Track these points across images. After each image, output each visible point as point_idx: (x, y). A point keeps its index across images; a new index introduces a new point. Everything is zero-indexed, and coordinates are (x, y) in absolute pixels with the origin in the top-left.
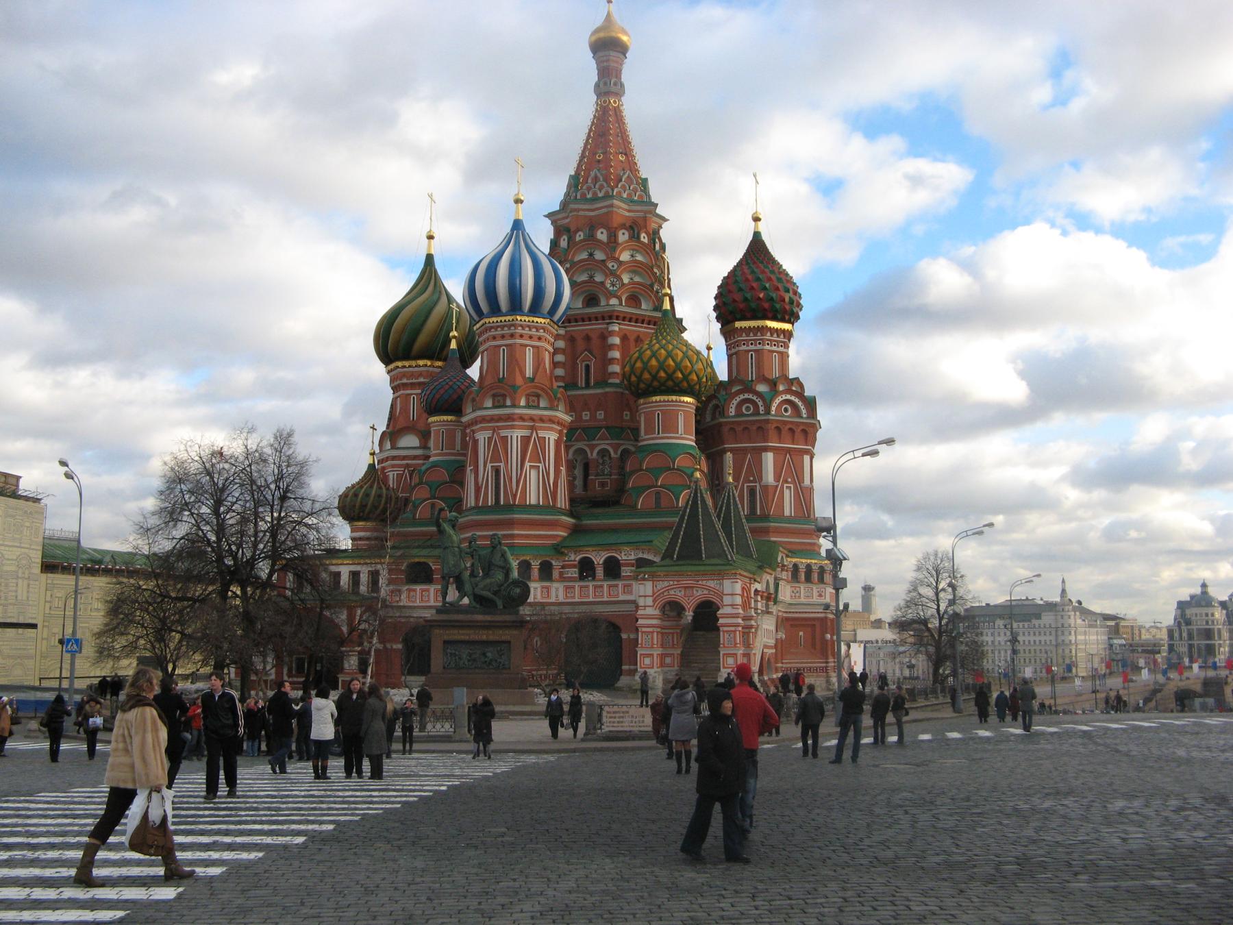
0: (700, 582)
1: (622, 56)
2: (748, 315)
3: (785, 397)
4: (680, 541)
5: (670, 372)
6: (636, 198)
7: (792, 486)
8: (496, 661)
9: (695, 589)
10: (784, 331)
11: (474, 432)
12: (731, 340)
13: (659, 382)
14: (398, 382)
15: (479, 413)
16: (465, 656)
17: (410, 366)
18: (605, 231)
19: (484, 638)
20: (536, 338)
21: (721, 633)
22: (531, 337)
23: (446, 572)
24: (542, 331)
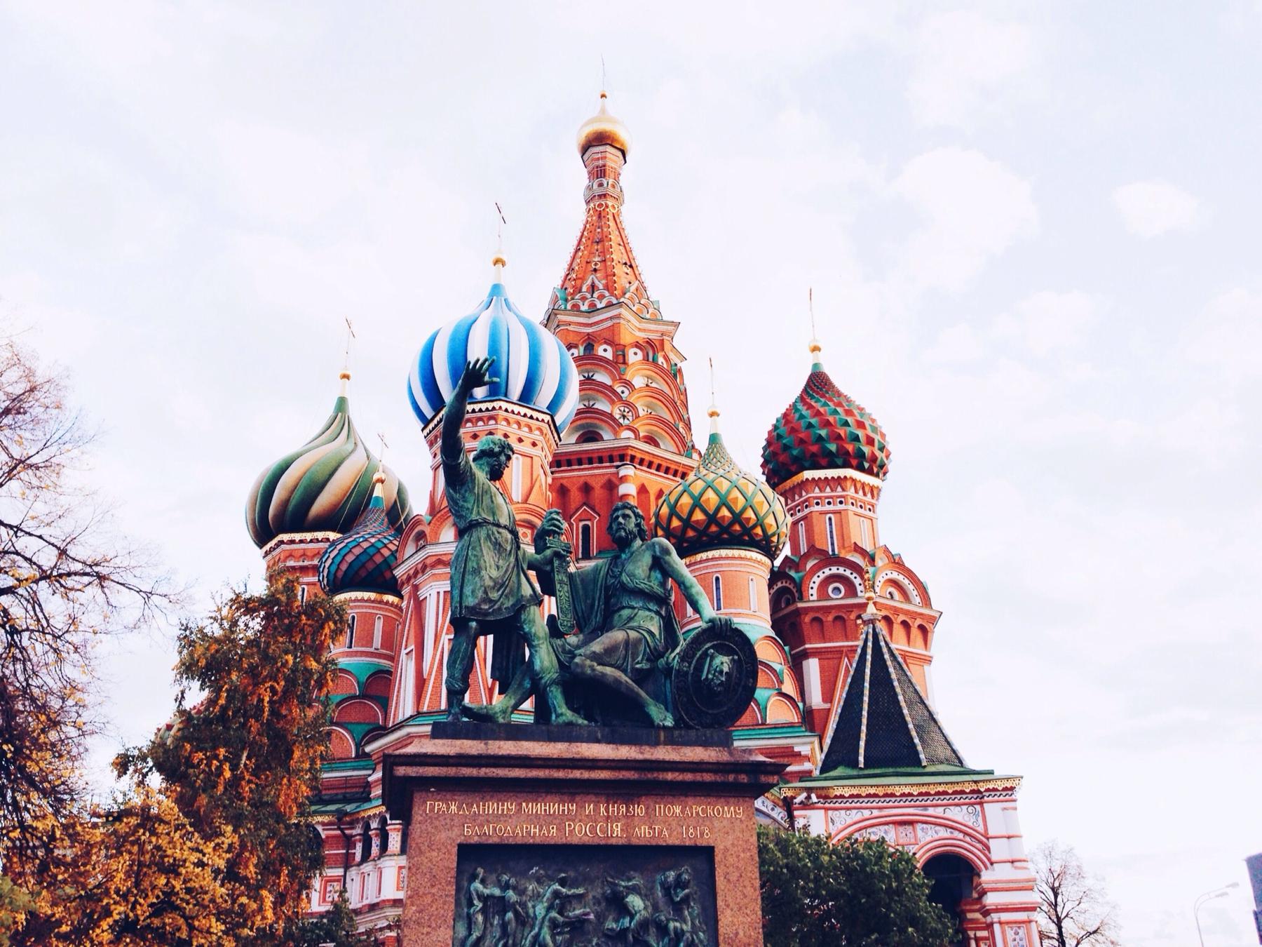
0: (931, 811)
1: (621, 157)
2: (823, 462)
3: (890, 576)
4: (864, 728)
5: (738, 510)
6: (648, 316)
8: (662, 930)
9: (919, 826)
10: (872, 489)
11: (416, 588)
13: (718, 525)
14: (281, 565)
15: (431, 550)
16: (540, 910)
17: (301, 541)
18: (609, 348)
19: (616, 833)
20: (527, 442)
21: (997, 927)
23: (470, 601)
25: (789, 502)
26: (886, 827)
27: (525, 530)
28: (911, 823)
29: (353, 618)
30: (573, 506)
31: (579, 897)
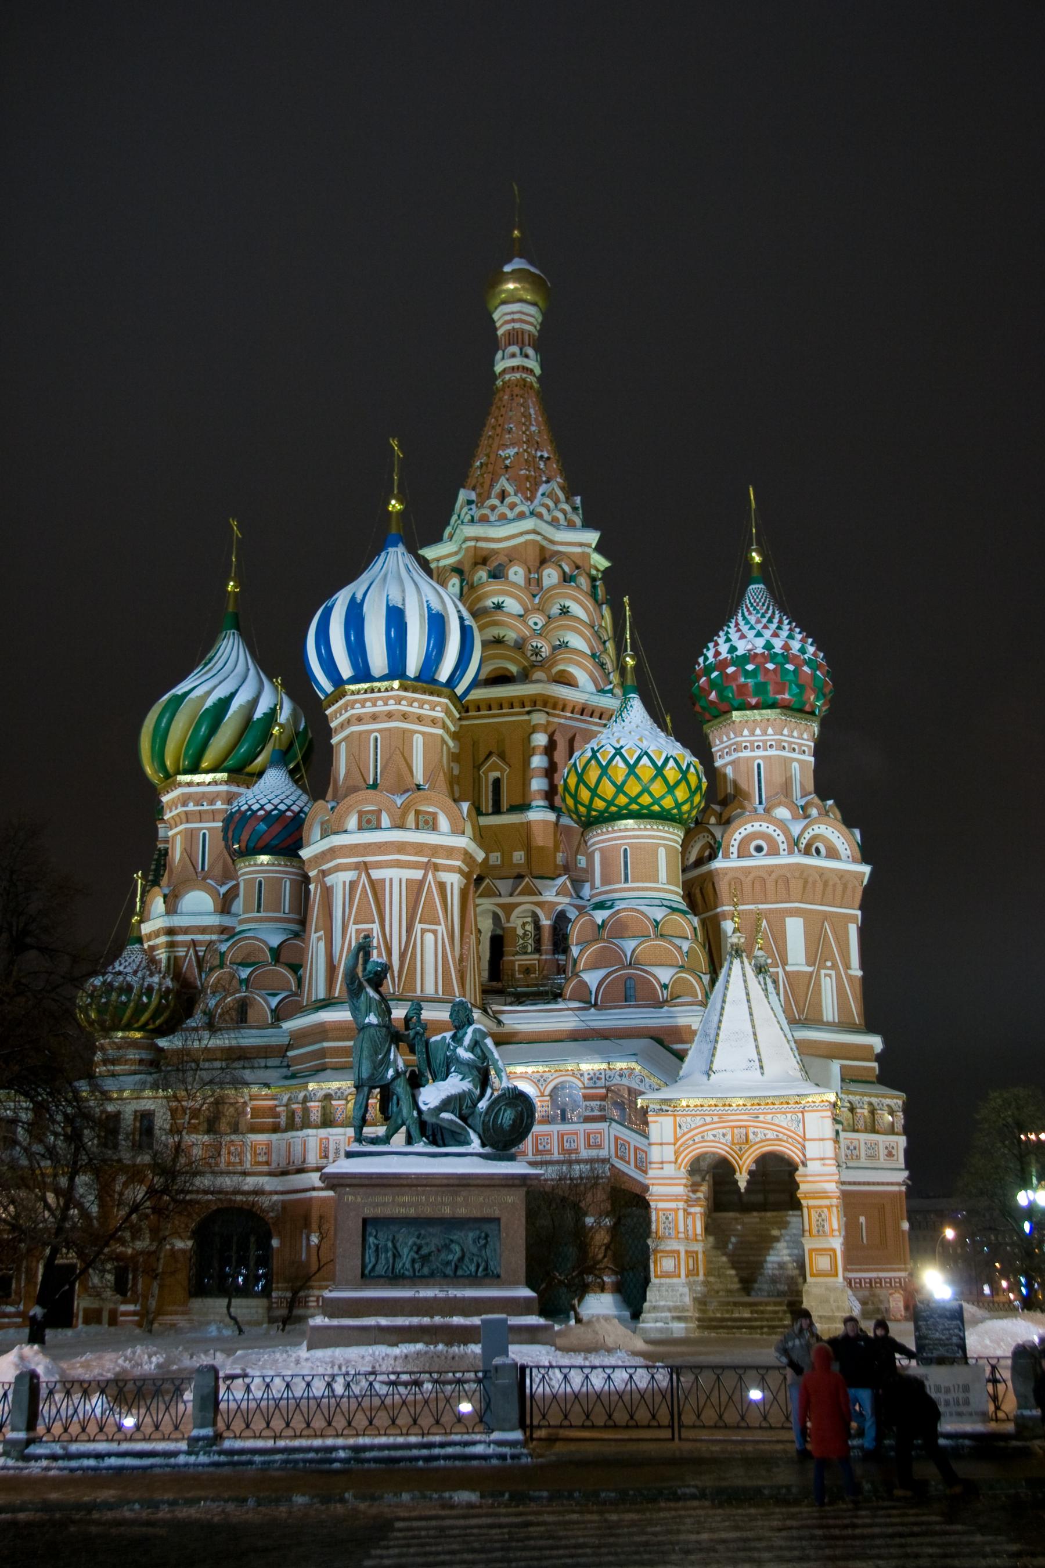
0: (761, 1118)
7: (833, 973)
8: (472, 1260)
9: (751, 1130)
11: (324, 873)
12: (722, 742)
13: (626, 794)
14: (180, 809)
16: (406, 1251)
17: (199, 784)
19: (447, 1212)
21: (805, 1210)
22: (420, 719)
24: (438, 708)
25: (718, 742)
26: (724, 1131)
27: (426, 817)
28: (746, 1127)
29: (260, 883)
30: (482, 758)
31: (427, 1244)
